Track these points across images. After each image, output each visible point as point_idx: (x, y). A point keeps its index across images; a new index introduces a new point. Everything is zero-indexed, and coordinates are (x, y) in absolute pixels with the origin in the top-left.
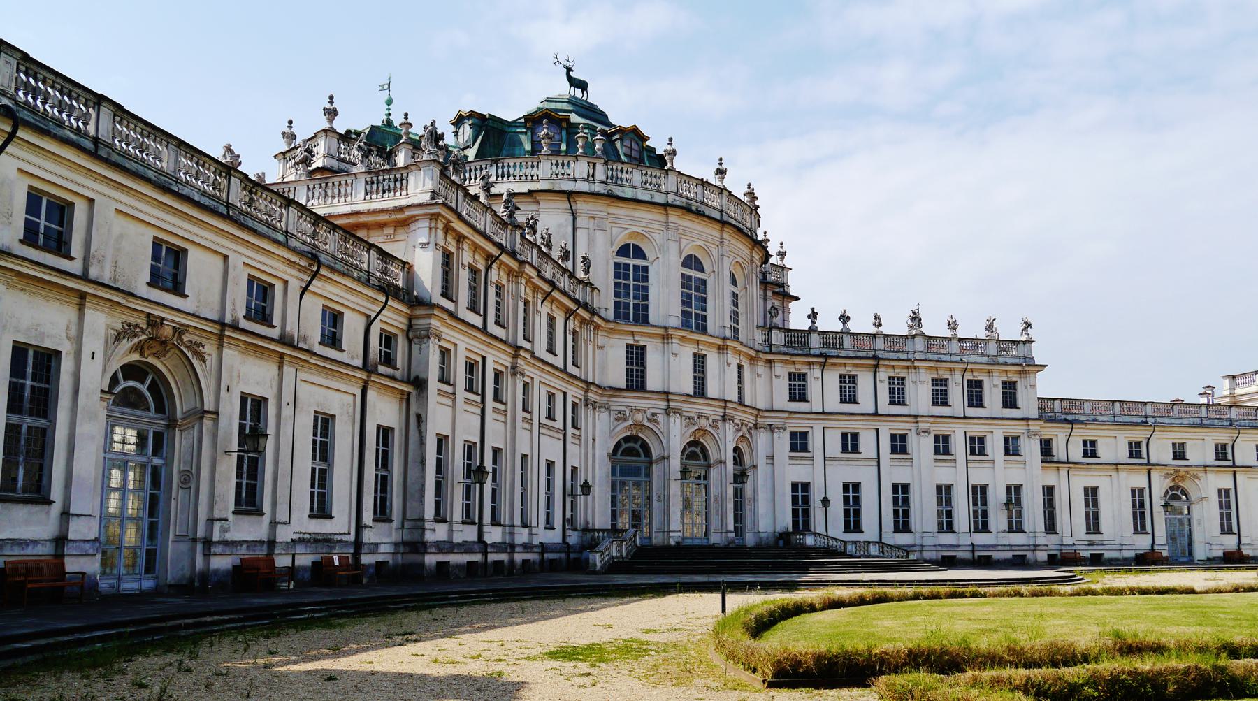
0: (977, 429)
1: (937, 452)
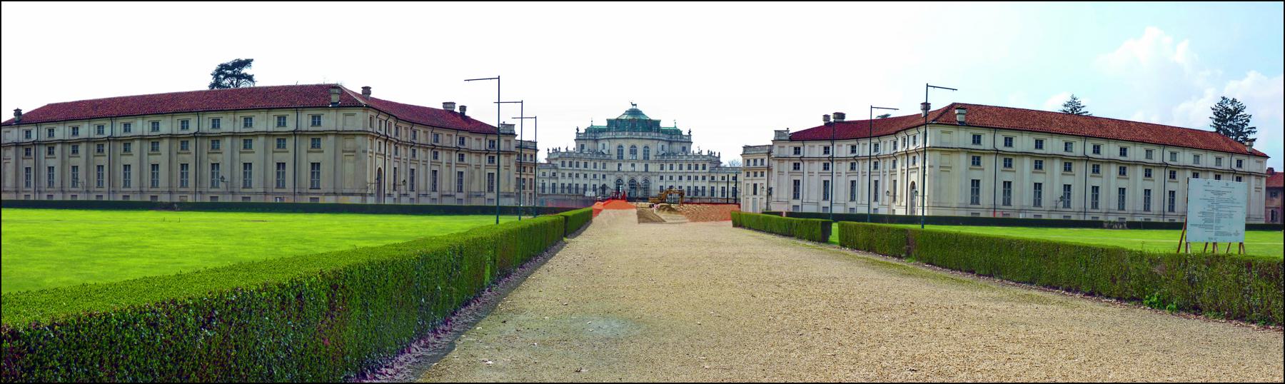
0: (697, 175)
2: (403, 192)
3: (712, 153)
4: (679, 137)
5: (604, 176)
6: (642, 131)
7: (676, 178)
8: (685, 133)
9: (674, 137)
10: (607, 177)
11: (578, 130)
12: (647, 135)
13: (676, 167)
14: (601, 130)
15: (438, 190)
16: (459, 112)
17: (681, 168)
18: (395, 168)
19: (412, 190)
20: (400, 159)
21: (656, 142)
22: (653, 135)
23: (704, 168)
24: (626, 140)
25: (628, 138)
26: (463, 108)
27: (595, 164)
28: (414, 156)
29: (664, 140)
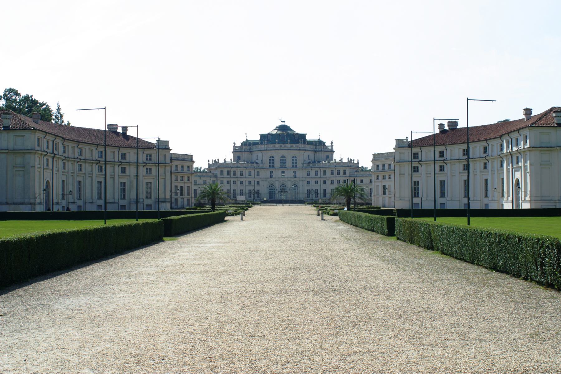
0: (338, 179)
1: (332, 183)
2: (71, 200)
3: (351, 160)
4: (322, 147)
5: (258, 183)
6: (290, 143)
7: (321, 182)
8: (328, 144)
9: (318, 147)
10: (260, 183)
11: (234, 144)
12: (295, 146)
13: (320, 173)
14: (255, 143)
15: (82, 198)
16: (121, 132)
17: (325, 174)
18: (63, 181)
19: (79, 198)
20: (68, 172)
21: (303, 152)
22: (300, 146)
23: (345, 173)
24: (277, 151)
25: (278, 150)
26: (125, 129)
27: (250, 173)
28: (81, 170)
29: (309, 151)
